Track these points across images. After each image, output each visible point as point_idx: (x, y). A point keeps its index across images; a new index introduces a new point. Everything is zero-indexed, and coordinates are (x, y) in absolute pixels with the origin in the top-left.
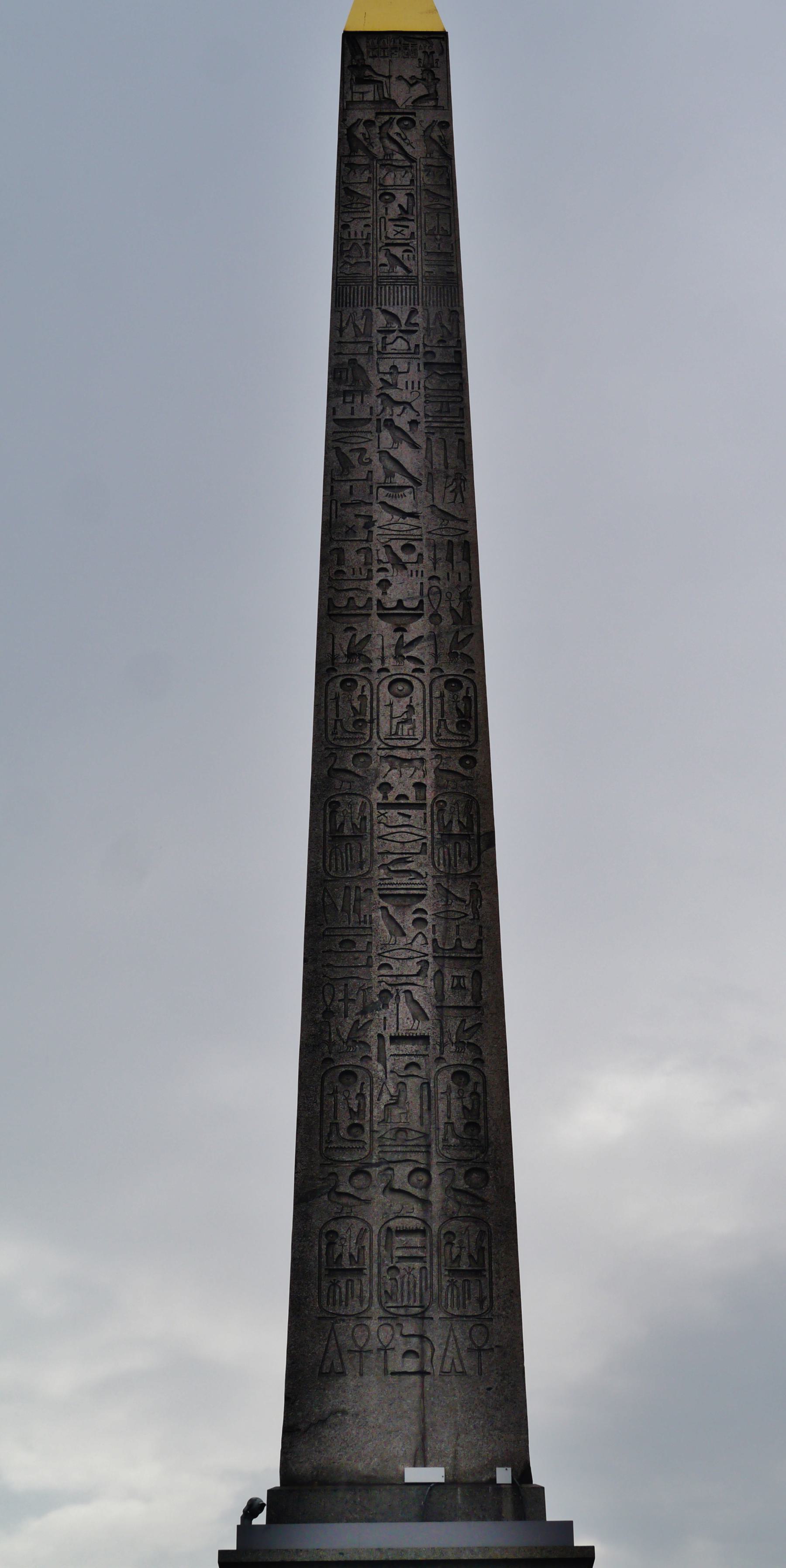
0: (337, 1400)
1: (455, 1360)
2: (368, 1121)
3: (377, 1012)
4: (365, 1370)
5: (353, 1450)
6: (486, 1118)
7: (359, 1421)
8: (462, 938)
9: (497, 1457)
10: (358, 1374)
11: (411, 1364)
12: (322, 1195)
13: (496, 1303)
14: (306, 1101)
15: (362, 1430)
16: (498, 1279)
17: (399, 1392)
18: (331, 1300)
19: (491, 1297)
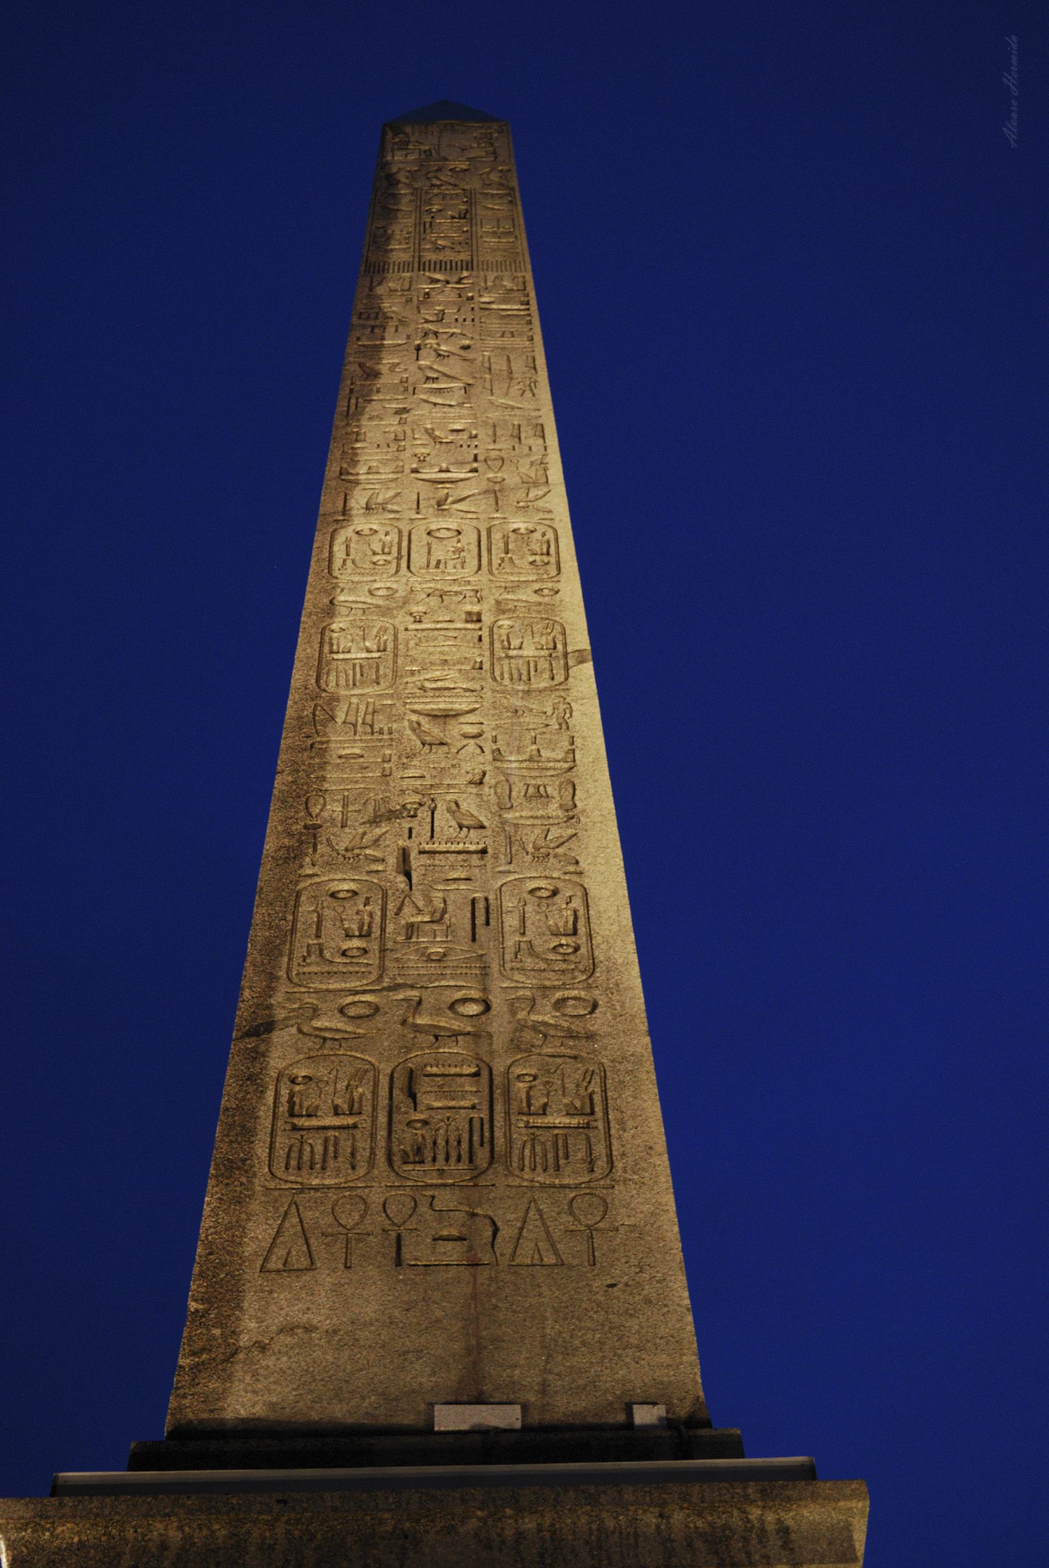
0: (296, 1308)
1: (540, 1244)
2: (376, 939)
3: (398, 820)
4: (354, 1260)
5: (324, 1386)
6: (590, 936)
7: (340, 1340)
8: (540, 747)
9: (633, 1390)
10: (341, 1266)
11: (452, 1252)
12: (287, 1027)
13: (619, 1165)
14: (266, 919)
15: (346, 1354)
16: (621, 1132)
17: (425, 1291)
18: (293, 1163)
19: (610, 1156)
